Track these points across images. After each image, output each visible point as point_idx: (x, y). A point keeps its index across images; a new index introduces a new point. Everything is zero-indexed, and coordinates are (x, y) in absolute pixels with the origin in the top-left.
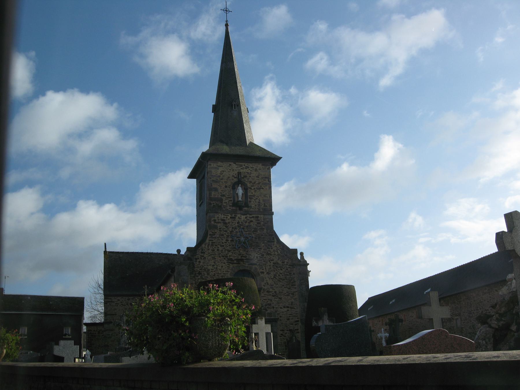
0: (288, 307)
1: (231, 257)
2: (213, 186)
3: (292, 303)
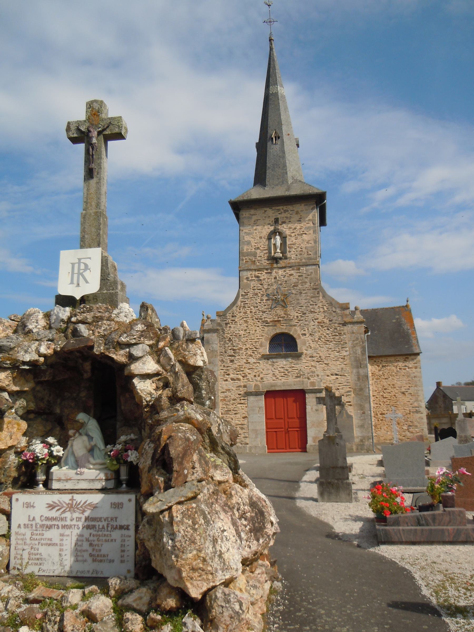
0: (337, 375)
1: (266, 319)
2: (246, 239)
3: (342, 369)
